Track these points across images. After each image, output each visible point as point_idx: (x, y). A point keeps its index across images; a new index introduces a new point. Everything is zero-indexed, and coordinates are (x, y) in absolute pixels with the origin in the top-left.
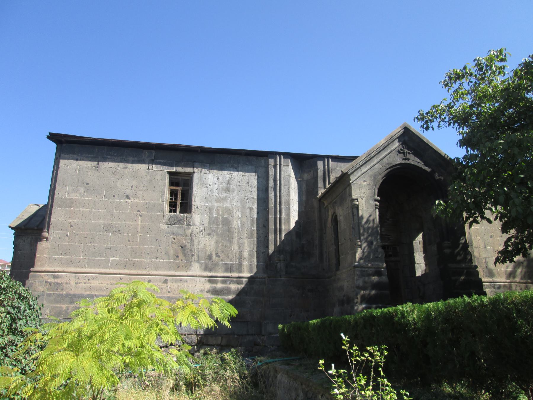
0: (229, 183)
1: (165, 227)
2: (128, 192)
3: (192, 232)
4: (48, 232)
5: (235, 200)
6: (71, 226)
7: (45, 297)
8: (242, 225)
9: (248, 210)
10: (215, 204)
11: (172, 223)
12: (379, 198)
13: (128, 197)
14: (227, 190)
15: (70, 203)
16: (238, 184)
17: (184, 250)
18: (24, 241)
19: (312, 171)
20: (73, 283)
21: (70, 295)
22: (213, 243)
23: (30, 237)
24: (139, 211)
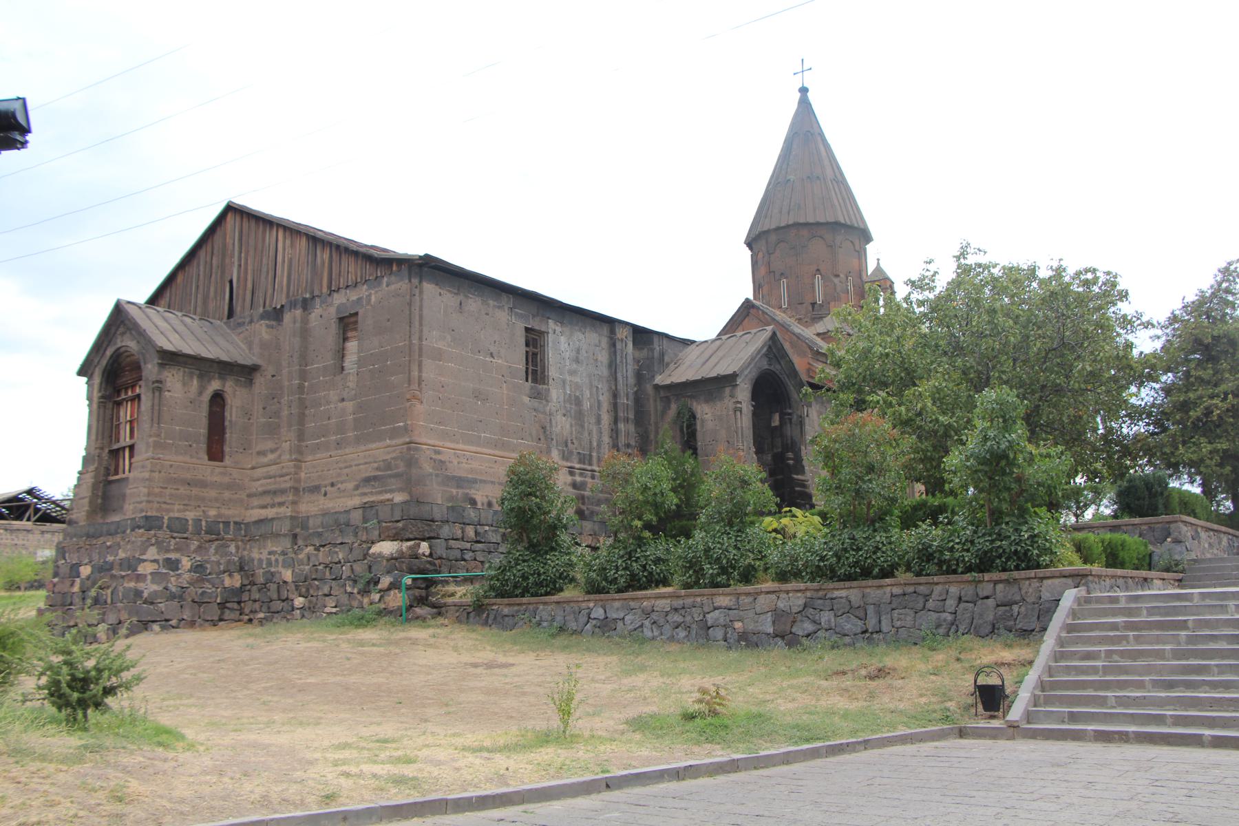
0: (578, 351)
1: (526, 399)
2: (492, 349)
3: (550, 410)
4: (420, 391)
5: (584, 375)
6: (443, 387)
7: (434, 477)
8: (591, 407)
9: (595, 389)
10: (568, 378)
11: (537, 395)
12: (754, 403)
13: (492, 355)
14: (577, 361)
15: (438, 355)
16: (585, 355)
17: (545, 432)
18: (173, 375)
19: (646, 350)
20: (455, 463)
21: (456, 477)
22: (568, 426)
23: (182, 369)
24: (503, 376)
